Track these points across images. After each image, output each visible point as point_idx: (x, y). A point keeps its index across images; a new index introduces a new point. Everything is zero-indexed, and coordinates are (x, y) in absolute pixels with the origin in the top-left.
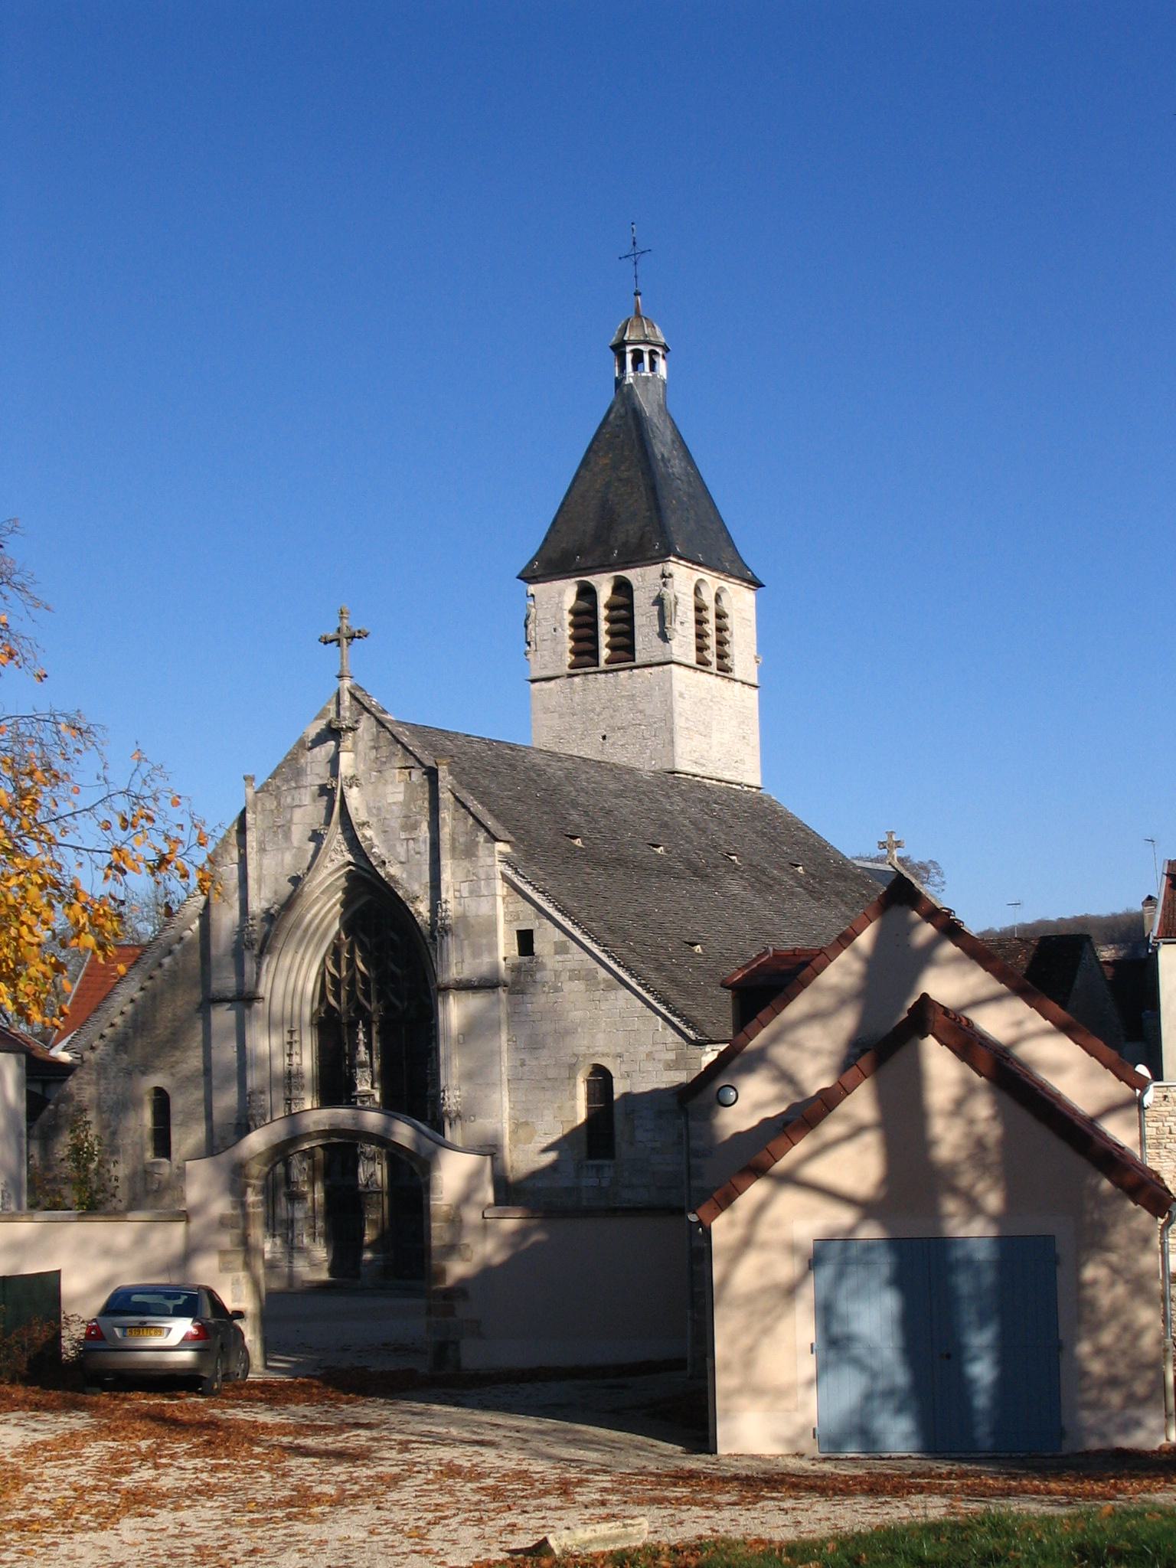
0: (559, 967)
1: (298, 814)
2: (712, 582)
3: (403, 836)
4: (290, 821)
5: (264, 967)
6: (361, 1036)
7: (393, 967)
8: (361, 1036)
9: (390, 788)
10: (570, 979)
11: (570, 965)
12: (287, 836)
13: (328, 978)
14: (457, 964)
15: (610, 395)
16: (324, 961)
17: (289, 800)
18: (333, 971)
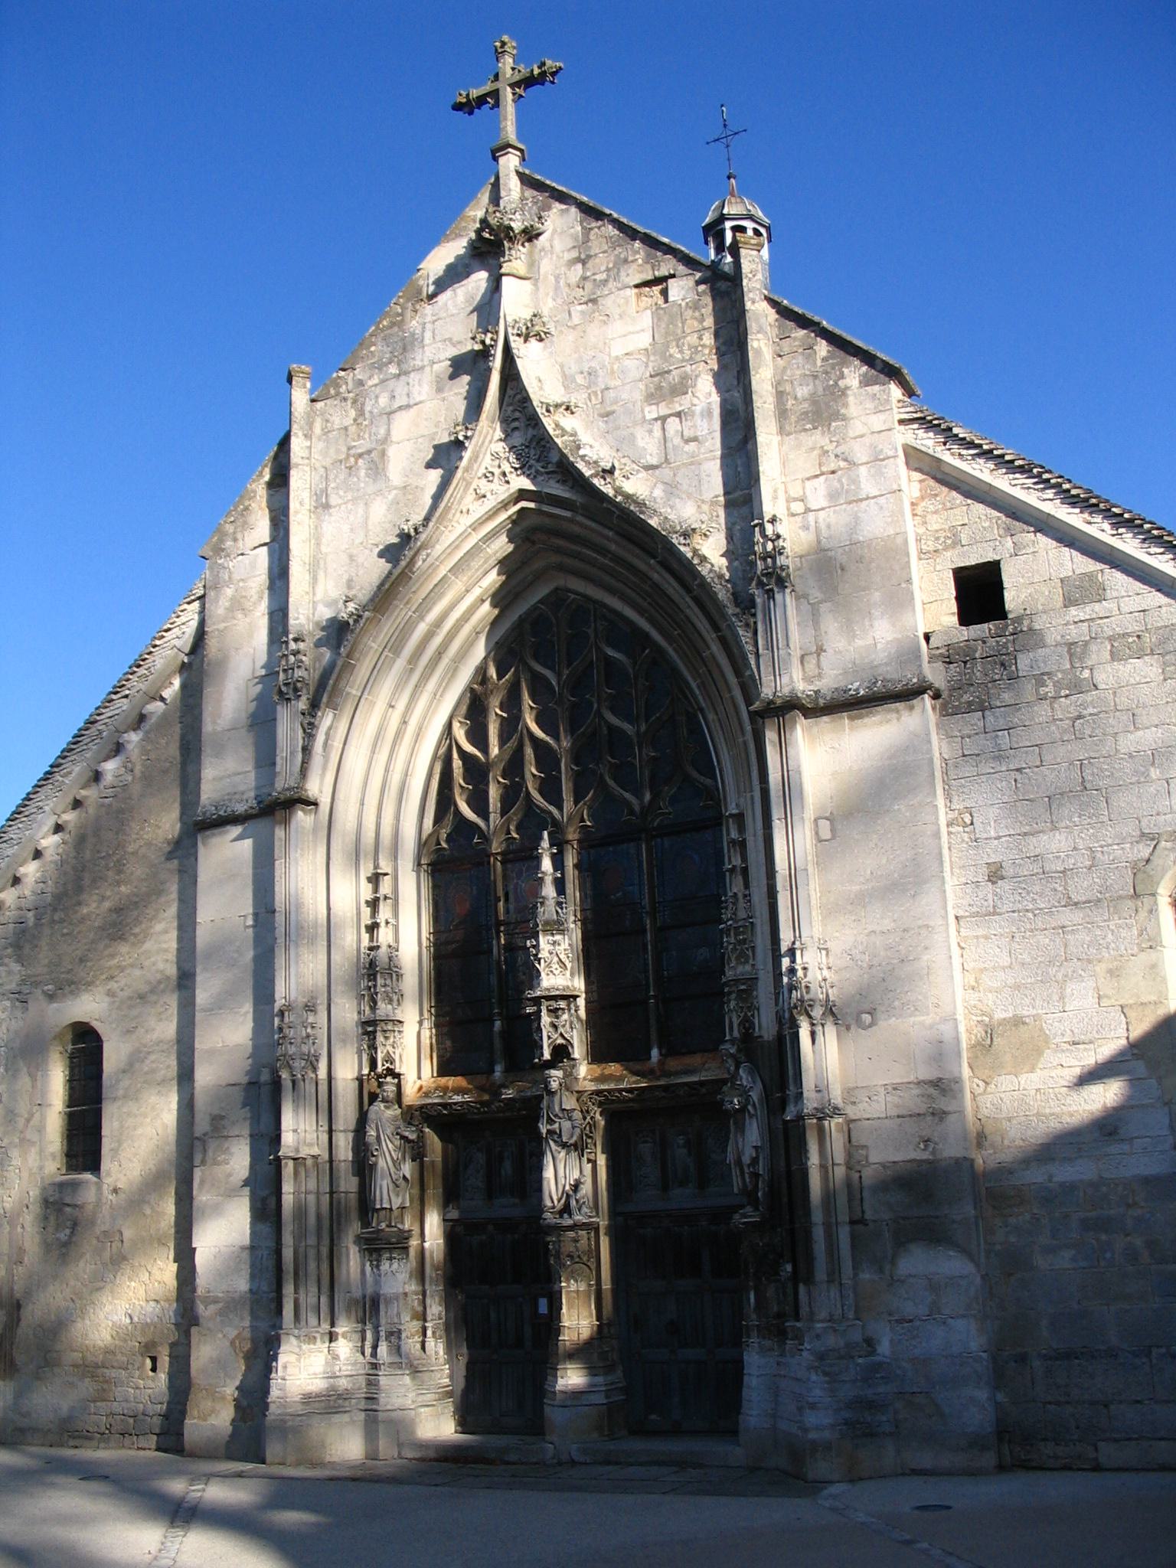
1: (402, 425)
3: (652, 412)
4: (386, 440)
5: (320, 738)
6: (547, 864)
8: (547, 864)
9: (617, 327)
10: (1114, 656)
12: (377, 467)
13: (457, 763)
14: (802, 653)
16: (449, 726)
17: (383, 401)
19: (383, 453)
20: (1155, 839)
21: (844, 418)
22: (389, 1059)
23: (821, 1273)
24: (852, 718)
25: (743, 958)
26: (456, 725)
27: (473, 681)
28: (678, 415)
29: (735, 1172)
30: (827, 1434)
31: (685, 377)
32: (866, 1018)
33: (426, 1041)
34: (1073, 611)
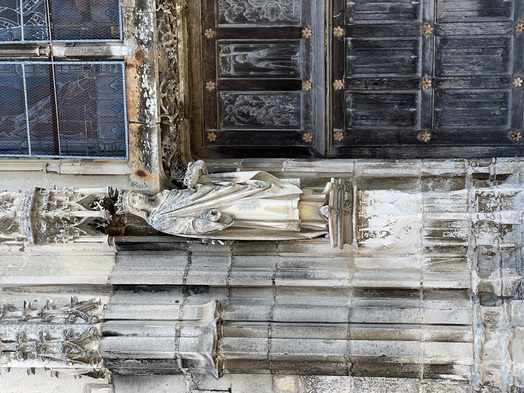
22: (90, 203)
33: (77, 168)
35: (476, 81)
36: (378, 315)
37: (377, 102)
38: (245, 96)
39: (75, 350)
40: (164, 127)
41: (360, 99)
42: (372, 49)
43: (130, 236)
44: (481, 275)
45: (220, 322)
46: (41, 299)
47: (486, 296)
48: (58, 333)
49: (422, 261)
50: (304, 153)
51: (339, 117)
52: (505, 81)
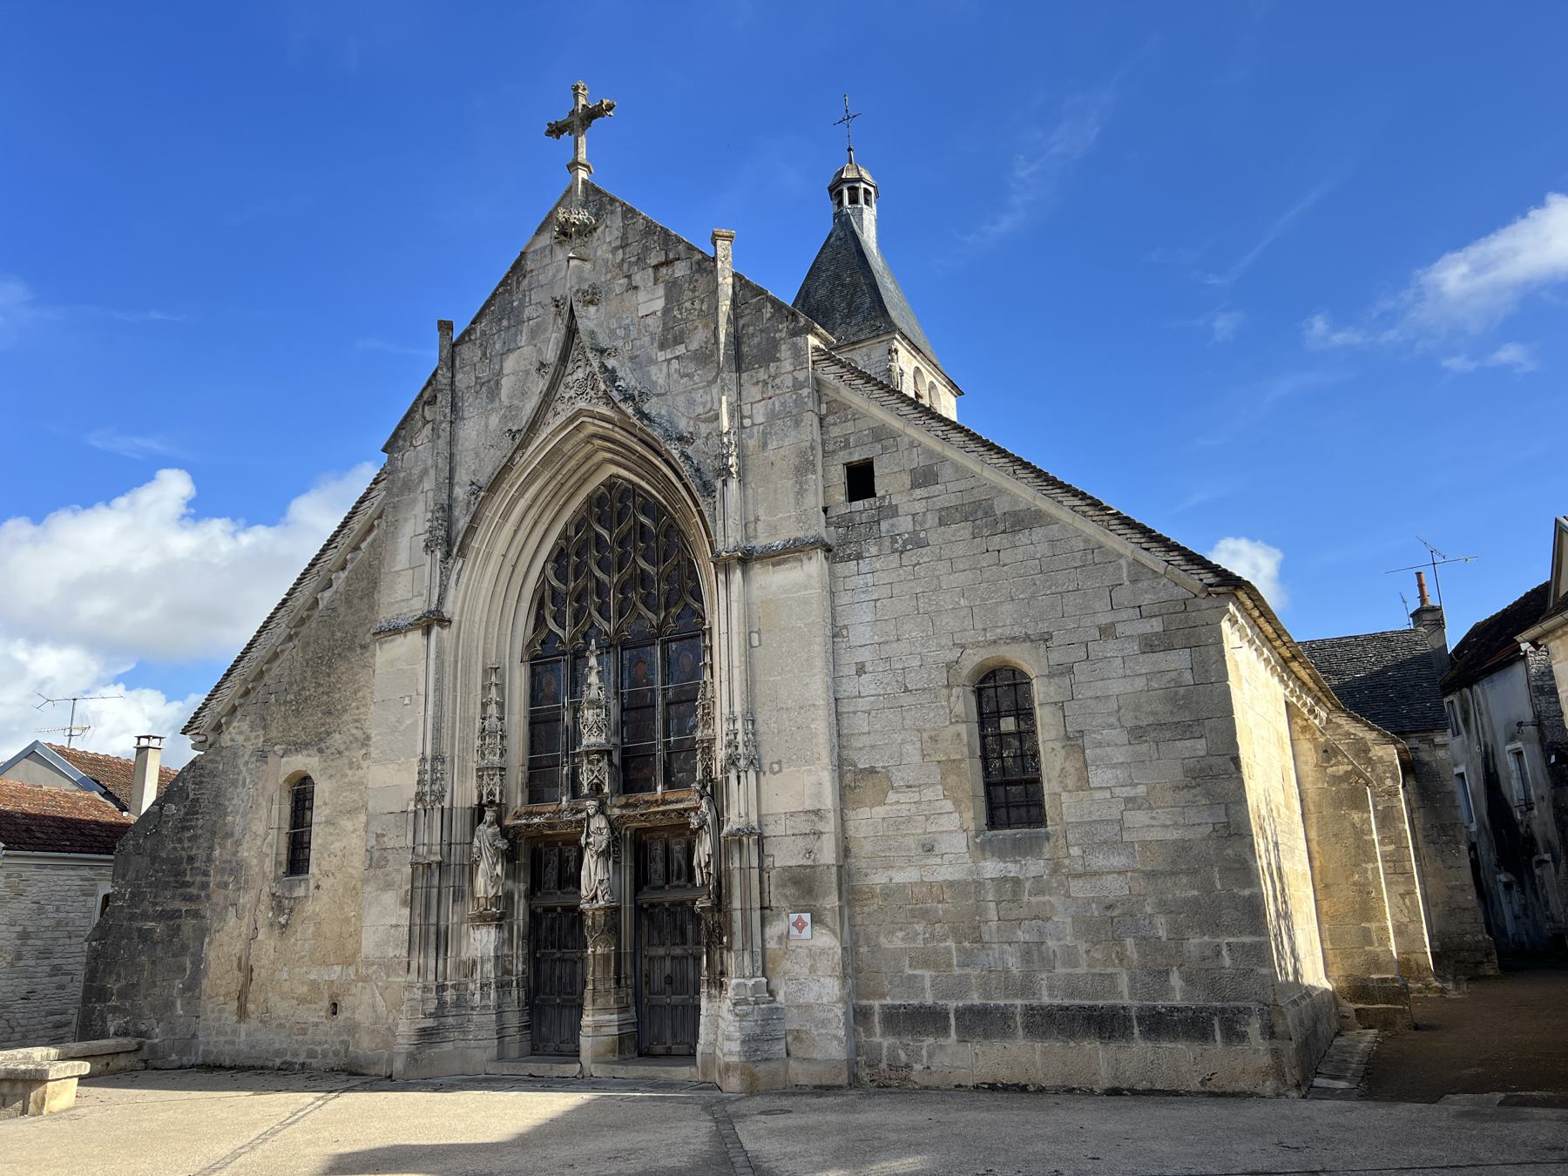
0: (919, 507)
1: (510, 364)
2: (928, 377)
3: (661, 356)
4: (500, 373)
5: (454, 577)
6: (593, 661)
7: (643, 564)
9: (642, 296)
11: (940, 502)
12: (494, 393)
13: (548, 593)
15: (828, 225)
18: (555, 583)
19: (498, 383)
20: (963, 647)
21: (779, 360)
22: (491, 793)
23: (738, 944)
24: (774, 565)
25: (707, 725)
26: (549, 566)
27: (560, 538)
28: (677, 358)
29: (697, 872)
30: (735, 1059)
31: (682, 331)
32: (776, 767)
34: (918, 491)
35: (560, 978)
36: (433, 938)
37: (552, 930)
38: (556, 859)
39: (420, 797)
40: (528, 826)
41: (553, 919)
42: (573, 925)
43: (478, 814)
44: (453, 986)
45: (429, 865)
46: (447, 777)
47: (441, 988)
48: (427, 788)
49: (464, 956)
50: (531, 894)
51: (548, 910)
52: (559, 993)
